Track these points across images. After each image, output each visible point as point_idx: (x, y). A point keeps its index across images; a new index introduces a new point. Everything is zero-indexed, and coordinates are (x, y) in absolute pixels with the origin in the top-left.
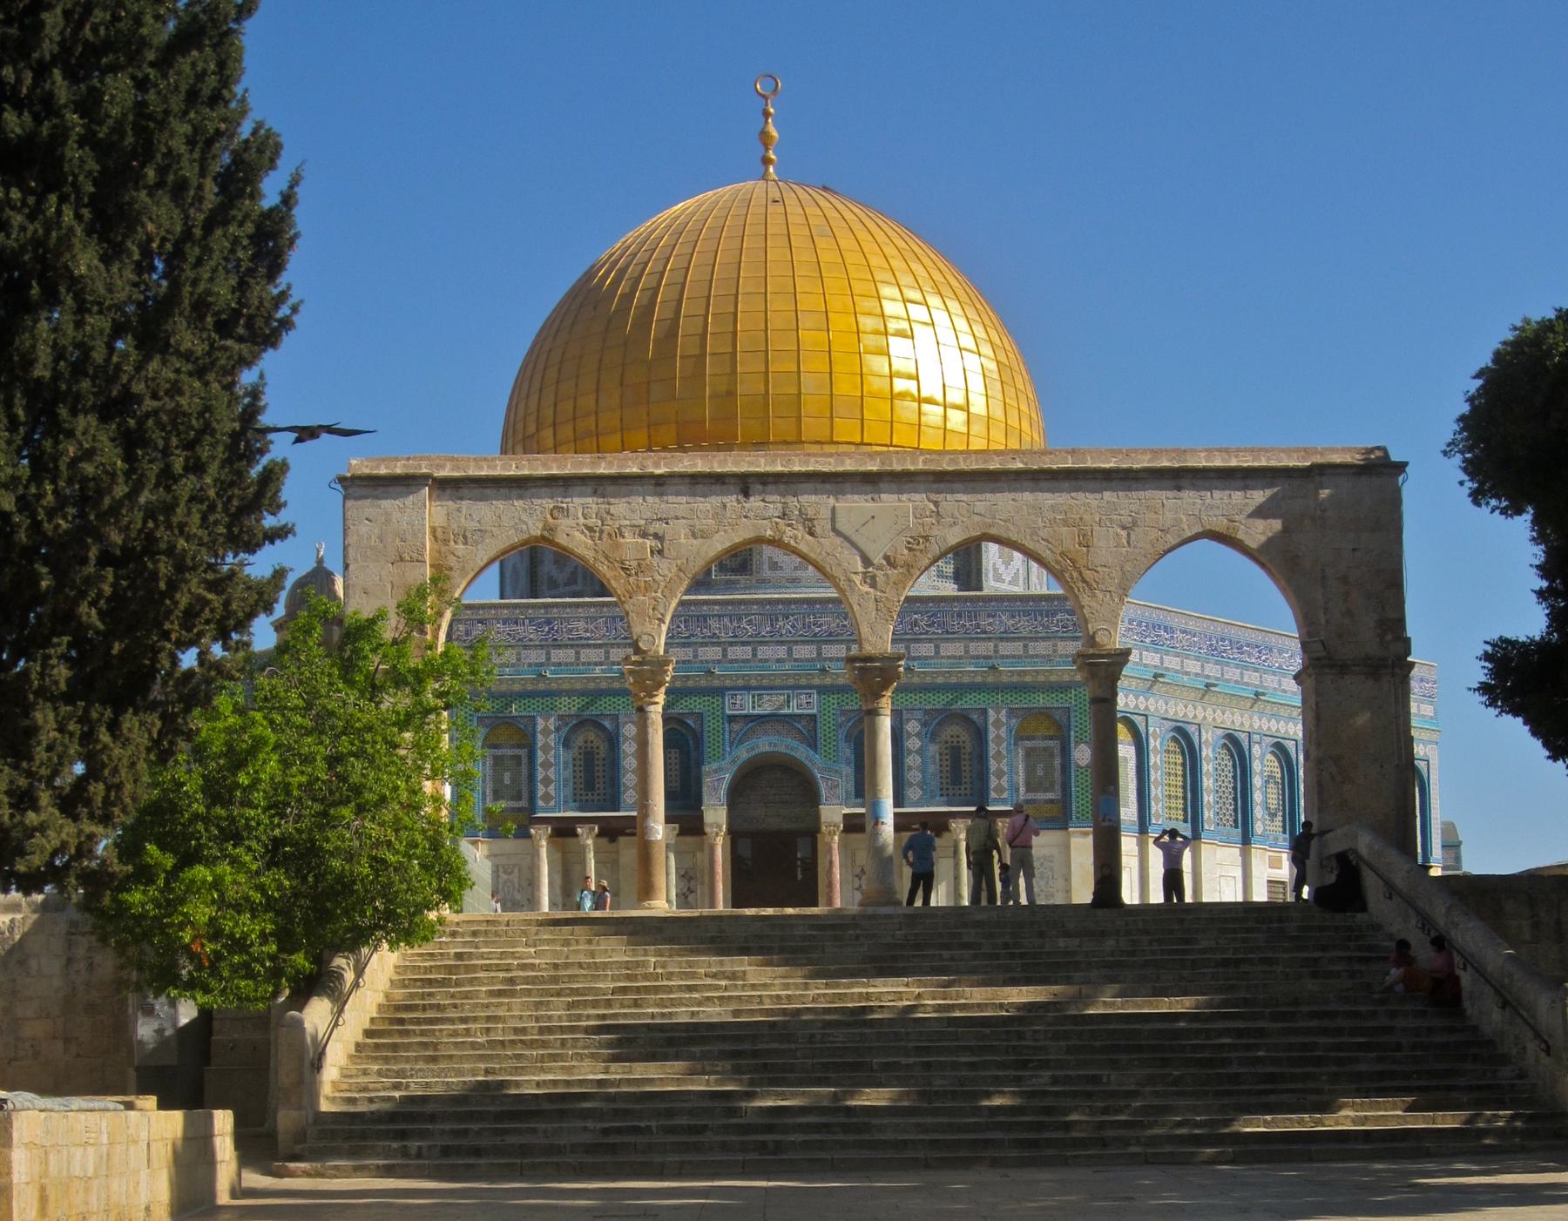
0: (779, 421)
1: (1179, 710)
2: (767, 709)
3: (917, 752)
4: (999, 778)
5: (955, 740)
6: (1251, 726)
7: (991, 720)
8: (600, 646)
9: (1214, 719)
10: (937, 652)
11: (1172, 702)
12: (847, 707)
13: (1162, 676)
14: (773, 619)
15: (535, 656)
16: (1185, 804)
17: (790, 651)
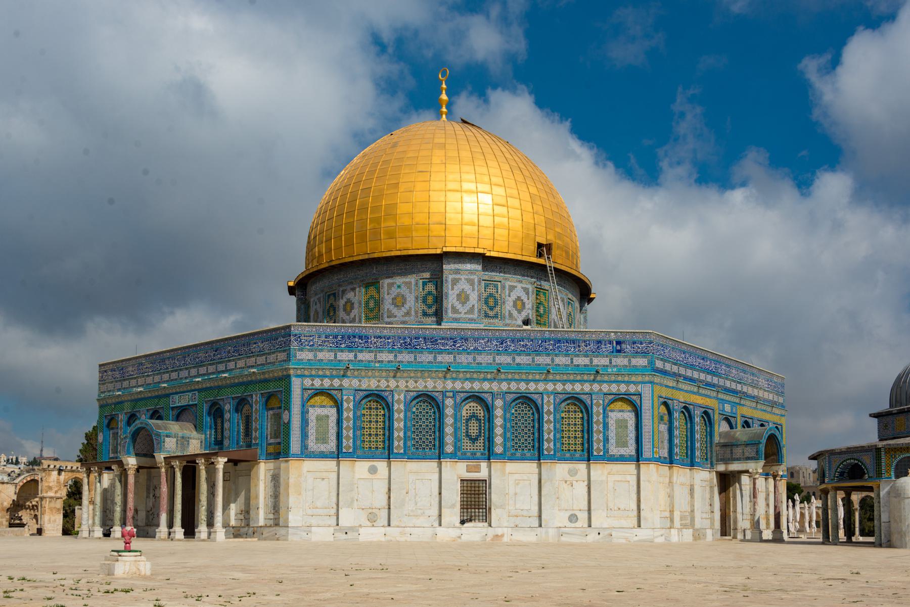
3: (229, 420)
7: (254, 400)
8: (135, 378)
9: (407, 386)
10: (236, 366)
14: (184, 357)
15: (118, 385)
17: (189, 372)
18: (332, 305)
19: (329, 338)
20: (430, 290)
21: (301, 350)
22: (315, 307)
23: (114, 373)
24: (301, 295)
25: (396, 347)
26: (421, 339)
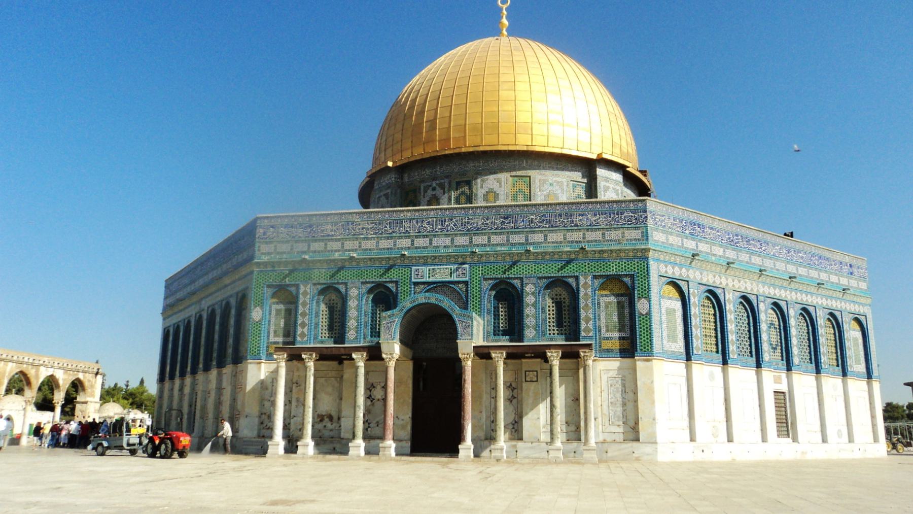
0: (487, 136)
1: (711, 279)
2: (438, 278)
3: (532, 305)
4: (587, 322)
5: (558, 297)
6: (758, 291)
8: (339, 240)
9: (733, 286)
10: (545, 239)
11: (705, 273)
12: (488, 276)
13: (697, 255)
14: (442, 222)
15: (302, 247)
16: (717, 341)
17: (452, 240)
18: (463, 193)
19: (676, 221)
20: (579, 194)
21: (656, 230)
22: (430, 192)
23: (291, 230)
24: (398, 178)
25: (724, 242)
26: (739, 237)
